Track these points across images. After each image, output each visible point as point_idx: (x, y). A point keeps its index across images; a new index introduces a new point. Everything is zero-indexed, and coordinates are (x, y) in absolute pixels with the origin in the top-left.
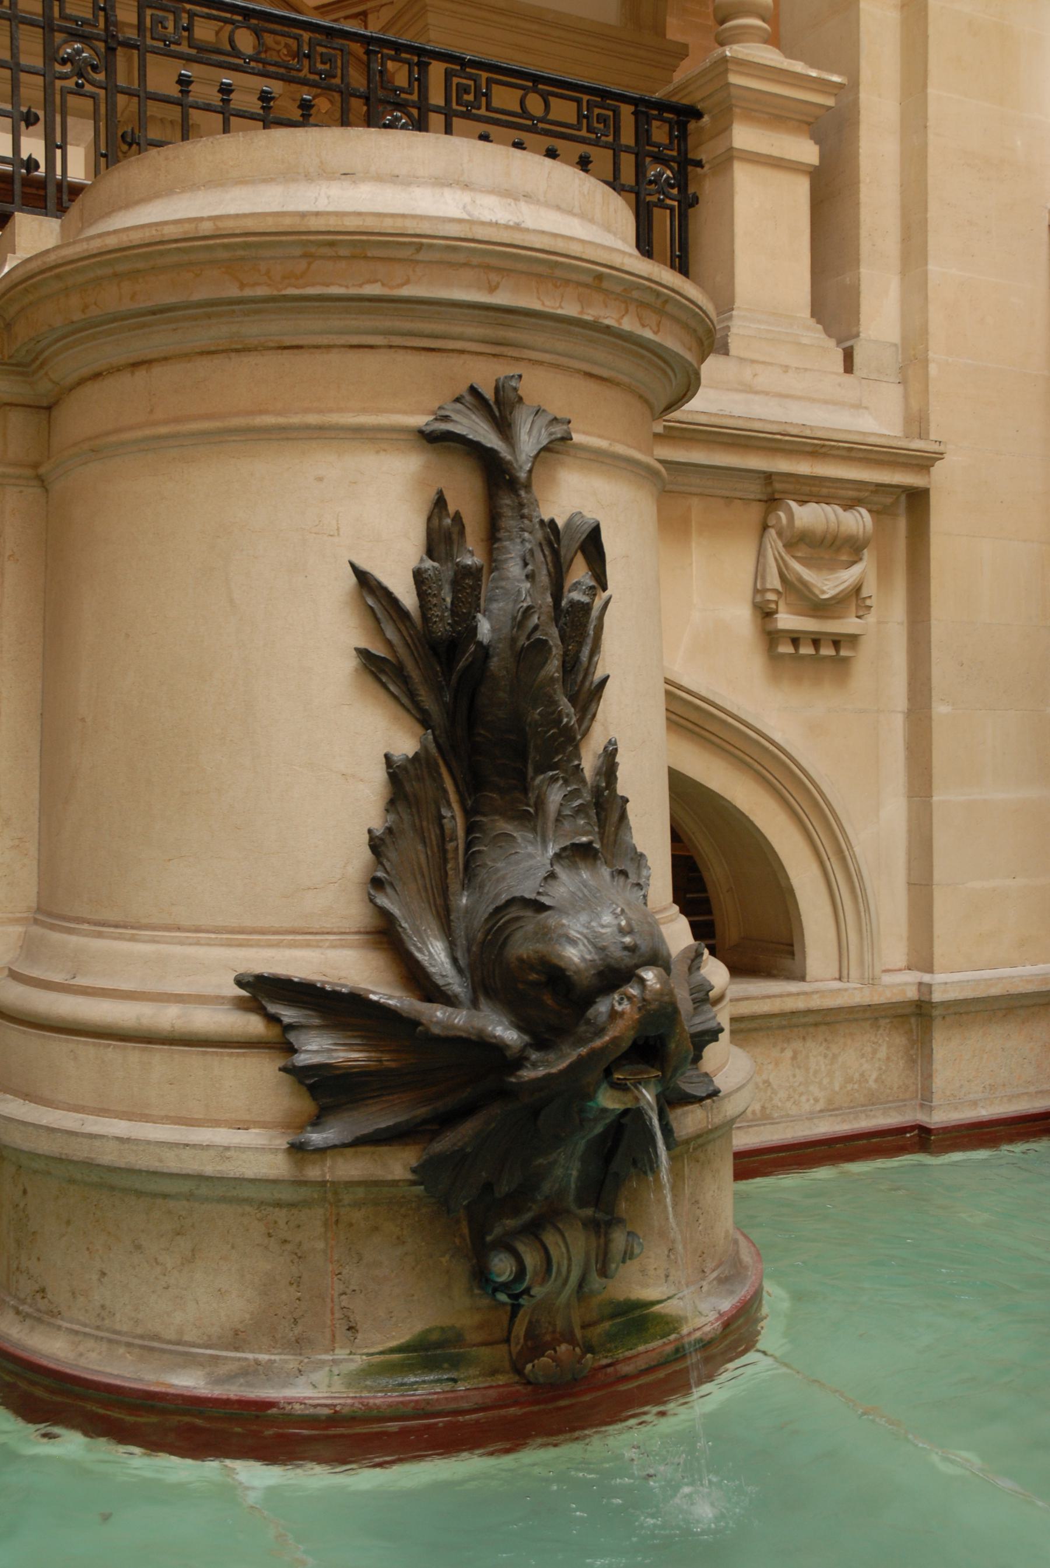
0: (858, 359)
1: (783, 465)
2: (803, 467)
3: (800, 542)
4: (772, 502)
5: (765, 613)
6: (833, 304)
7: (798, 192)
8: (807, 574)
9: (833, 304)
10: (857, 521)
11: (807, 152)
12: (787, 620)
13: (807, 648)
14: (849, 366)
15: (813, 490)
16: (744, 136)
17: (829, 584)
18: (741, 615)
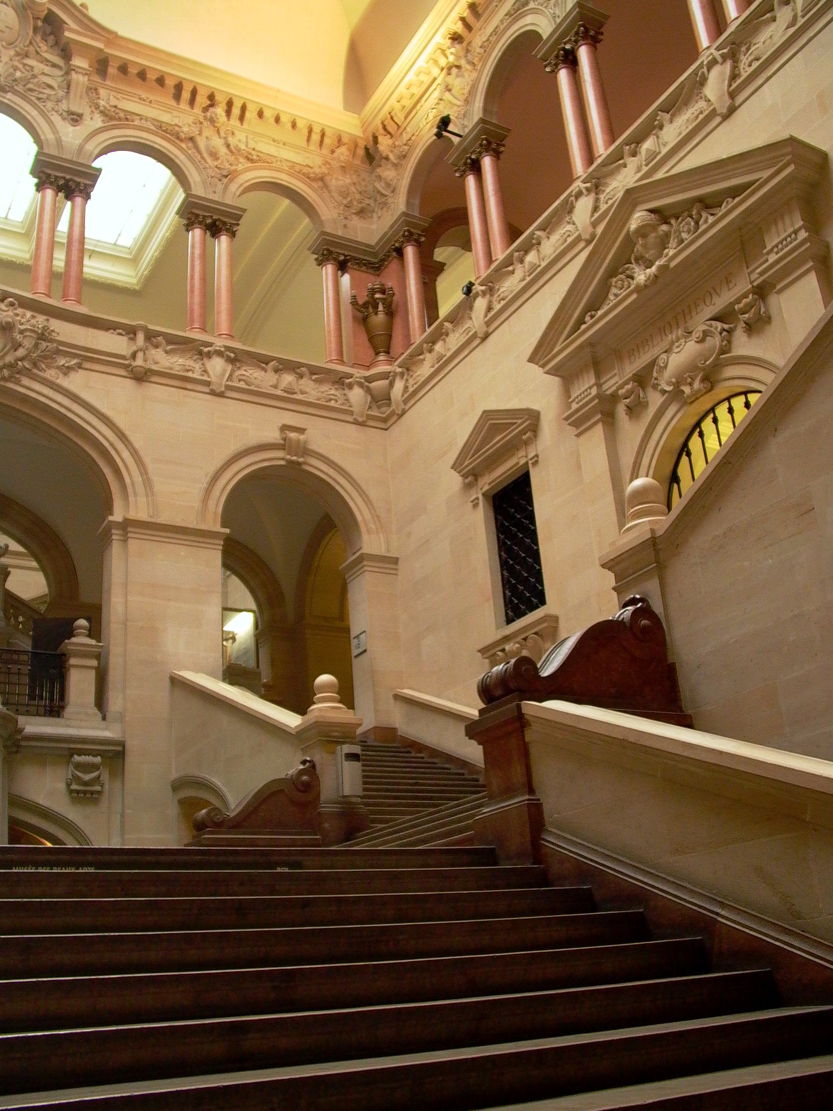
0: (107, 716)
1: (72, 746)
2: (79, 746)
3: (78, 766)
4: (72, 756)
5: (68, 785)
6: (100, 702)
7: (92, 674)
8: (79, 774)
9: (100, 702)
10: (98, 759)
11: (94, 663)
12: (74, 787)
13: (85, 794)
14: (104, 718)
15: (81, 752)
16: (73, 661)
17: (87, 777)
18: (62, 786)
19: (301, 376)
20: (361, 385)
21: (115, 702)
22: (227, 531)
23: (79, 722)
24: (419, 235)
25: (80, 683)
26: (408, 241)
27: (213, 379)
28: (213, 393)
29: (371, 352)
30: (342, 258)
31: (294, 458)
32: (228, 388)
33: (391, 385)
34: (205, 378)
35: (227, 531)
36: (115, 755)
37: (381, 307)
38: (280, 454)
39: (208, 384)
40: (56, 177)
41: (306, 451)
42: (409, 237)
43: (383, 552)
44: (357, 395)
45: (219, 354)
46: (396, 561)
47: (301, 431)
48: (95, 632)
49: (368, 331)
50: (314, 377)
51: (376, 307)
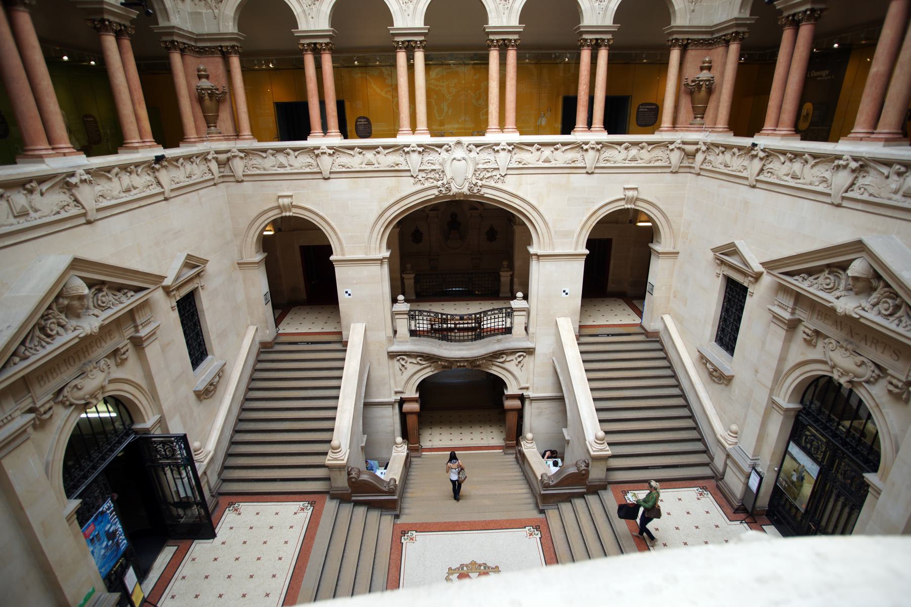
9: (526, 329)
19: (642, 148)
20: (679, 148)
21: (531, 330)
22: (587, 252)
23: (516, 340)
24: (744, 33)
25: (519, 321)
26: (734, 40)
27: (588, 166)
28: (587, 173)
29: (692, 116)
30: (685, 42)
31: (629, 206)
32: (596, 168)
33: (697, 150)
34: (582, 165)
35: (587, 252)
36: (530, 352)
37: (703, 89)
38: (623, 203)
39: (585, 168)
40: (497, 41)
41: (637, 199)
42: (736, 36)
43: (671, 250)
44: (676, 157)
45: (593, 148)
46: (678, 253)
47: (636, 189)
48: (526, 297)
49: (693, 102)
50: (651, 147)
51: (699, 87)
